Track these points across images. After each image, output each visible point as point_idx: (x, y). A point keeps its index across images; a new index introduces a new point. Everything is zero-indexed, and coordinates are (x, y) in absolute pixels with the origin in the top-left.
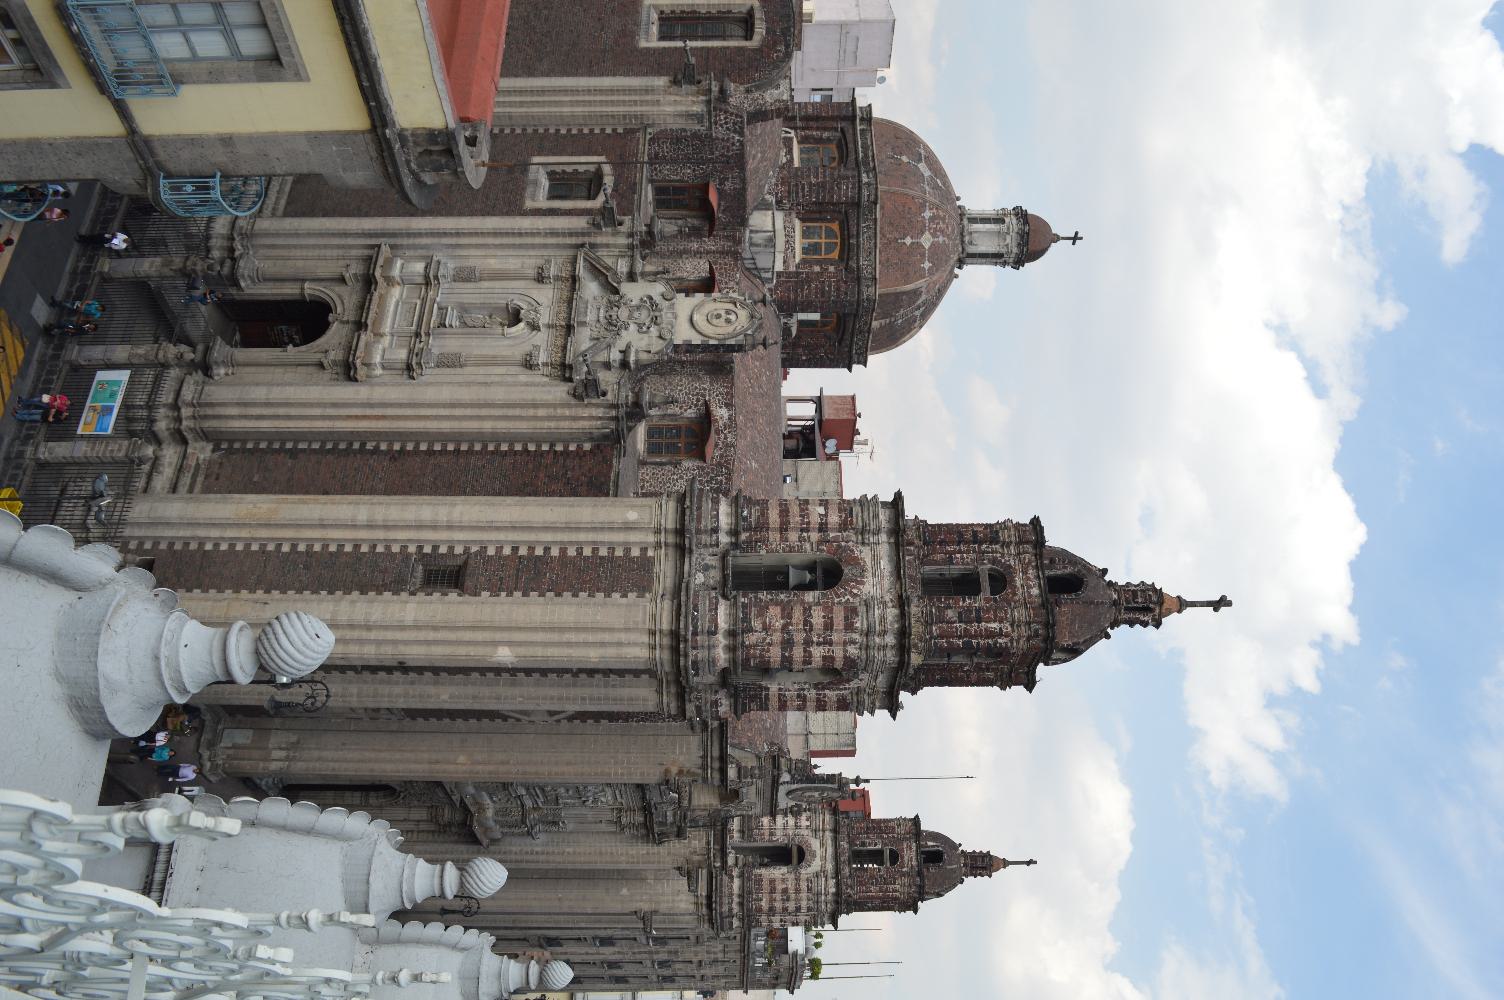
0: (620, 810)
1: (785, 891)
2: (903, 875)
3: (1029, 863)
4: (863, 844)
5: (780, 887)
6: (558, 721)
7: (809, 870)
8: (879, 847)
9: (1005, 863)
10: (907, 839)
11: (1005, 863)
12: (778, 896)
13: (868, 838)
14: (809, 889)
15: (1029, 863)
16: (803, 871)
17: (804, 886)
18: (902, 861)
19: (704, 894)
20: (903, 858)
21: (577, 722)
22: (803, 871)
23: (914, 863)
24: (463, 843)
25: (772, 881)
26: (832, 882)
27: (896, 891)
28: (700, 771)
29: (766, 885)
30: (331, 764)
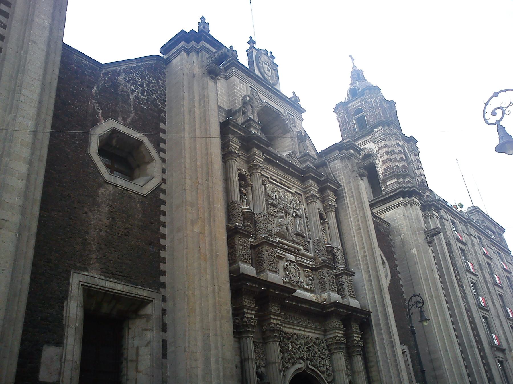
0: (307, 198)
1: (387, 153)
3: (351, 56)
5: (386, 157)
6: (164, 161)
7: (373, 148)
8: (354, 121)
9: (354, 66)
10: (347, 109)
11: (354, 66)
12: (393, 157)
13: (350, 128)
14: (383, 140)
15: (351, 56)
16: (375, 151)
17: (382, 143)
18: (359, 106)
19: (401, 199)
21: (162, 145)
22: (375, 150)
24: (373, 339)
25: (384, 162)
26: (375, 130)
27: (375, 100)
28: (200, 54)
29: (386, 166)
30: (213, 366)
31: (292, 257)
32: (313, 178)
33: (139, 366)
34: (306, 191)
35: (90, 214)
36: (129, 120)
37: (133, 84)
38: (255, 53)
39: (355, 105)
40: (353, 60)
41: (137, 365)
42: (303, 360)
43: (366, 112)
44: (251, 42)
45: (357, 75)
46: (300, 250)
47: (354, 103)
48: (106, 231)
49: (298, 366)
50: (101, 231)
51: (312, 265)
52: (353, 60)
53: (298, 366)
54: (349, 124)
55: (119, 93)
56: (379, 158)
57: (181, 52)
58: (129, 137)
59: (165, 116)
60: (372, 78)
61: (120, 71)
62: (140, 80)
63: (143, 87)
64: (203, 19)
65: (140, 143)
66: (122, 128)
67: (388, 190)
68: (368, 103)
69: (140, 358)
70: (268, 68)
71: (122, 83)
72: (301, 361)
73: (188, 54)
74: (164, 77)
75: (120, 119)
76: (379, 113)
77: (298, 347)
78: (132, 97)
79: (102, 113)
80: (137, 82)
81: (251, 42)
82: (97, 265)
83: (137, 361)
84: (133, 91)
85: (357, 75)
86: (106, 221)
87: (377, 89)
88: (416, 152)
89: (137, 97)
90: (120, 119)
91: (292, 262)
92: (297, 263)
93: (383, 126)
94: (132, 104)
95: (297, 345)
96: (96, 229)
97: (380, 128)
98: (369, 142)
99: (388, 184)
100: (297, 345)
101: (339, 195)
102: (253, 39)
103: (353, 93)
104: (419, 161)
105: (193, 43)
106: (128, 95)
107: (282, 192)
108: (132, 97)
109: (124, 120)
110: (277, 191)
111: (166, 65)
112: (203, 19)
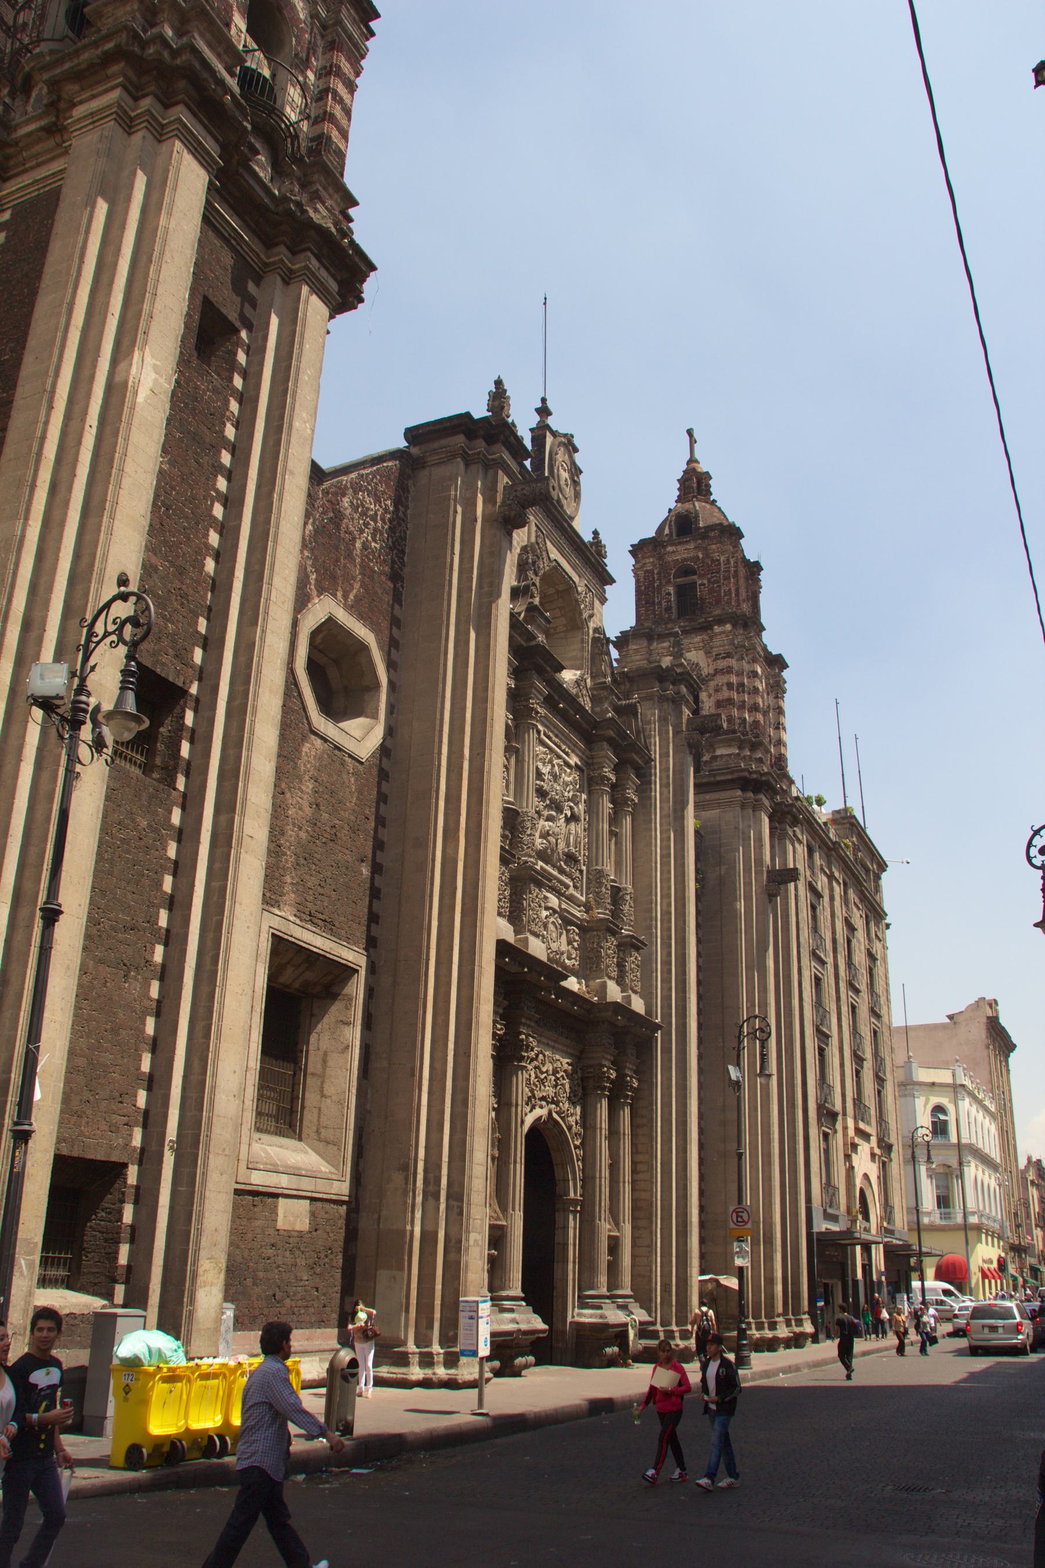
2: (707, 555)
3: (690, 433)
4: (668, 609)
5: (725, 694)
7: (703, 664)
8: (671, 589)
9: (692, 460)
10: (661, 558)
11: (692, 460)
13: (660, 603)
15: (690, 433)
16: (705, 672)
19: (739, 793)
20: (685, 560)
22: (705, 672)
23: (691, 546)
26: (717, 629)
27: (728, 561)
28: (491, 472)
31: (554, 901)
32: (610, 741)
33: (326, 1086)
34: (593, 764)
35: (288, 795)
36: (351, 597)
37: (364, 514)
38: (549, 439)
39: (681, 552)
40: (692, 441)
41: (322, 1083)
42: (548, 1103)
43: (701, 576)
44: (544, 411)
45: (695, 484)
46: (567, 887)
47: (679, 548)
48: (307, 831)
49: (538, 1112)
50: (300, 829)
51: (581, 920)
52: (692, 441)
53: (538, 1112)
54: (659, 592)
55: (342, 535)
56: (711, 691)
57: (454, 457)
58: (348, 634)
59: (402, 587)
60: (730, 500)
61: (346, 485)
62: (372, 506)
63: (376, 522)
64: (499, 383)
65: (364, 648)
66: (343, 617)
67: (715, 765)
68: (713, 561)
69: (328, 1071)
70: (566, 480)
71: (348, 512)
72: (544, 1103)
73: (467, 465)
74: (407, 499)
75: (339, 594)
76: (730, 590)
77: (543, 1076)
78: (358, 545)
79: (316, 580)
80: (368, 509)
81: (544, 411)
82: (293, 895)
83: (322, 1077)
84: (362, 532)
85: (695, 484)
86: (308, 811)
87: (734, 533)
88: (777, 688)
89: (365, 546)
90: (339, 594)
91: (555, 911)
92: (562, 914)
93: (734, 626)
94: (358, 560)
95: (542, 1073)
96: (294, 824)
97: (728, 627)
98: (697, 649)
99: (719, 752)
100: (542, 1073)
101: (644, 774)
102: (549, 404)
103: (681, 525)
104: (780, 711)
105: (480, 445)
106: (354, 539)
107: (558, 764)
108: (358, 545)
109: (345, 596)
110: (551, 761)
111: (413, 469)
112: (499, 383)
